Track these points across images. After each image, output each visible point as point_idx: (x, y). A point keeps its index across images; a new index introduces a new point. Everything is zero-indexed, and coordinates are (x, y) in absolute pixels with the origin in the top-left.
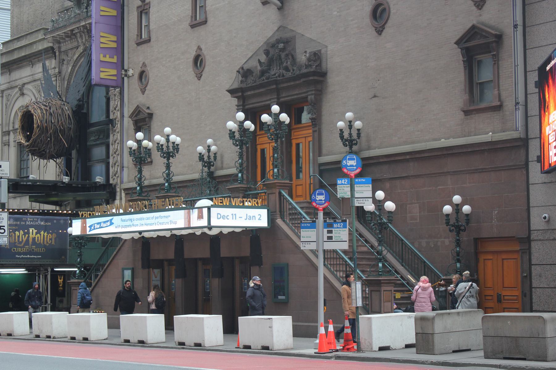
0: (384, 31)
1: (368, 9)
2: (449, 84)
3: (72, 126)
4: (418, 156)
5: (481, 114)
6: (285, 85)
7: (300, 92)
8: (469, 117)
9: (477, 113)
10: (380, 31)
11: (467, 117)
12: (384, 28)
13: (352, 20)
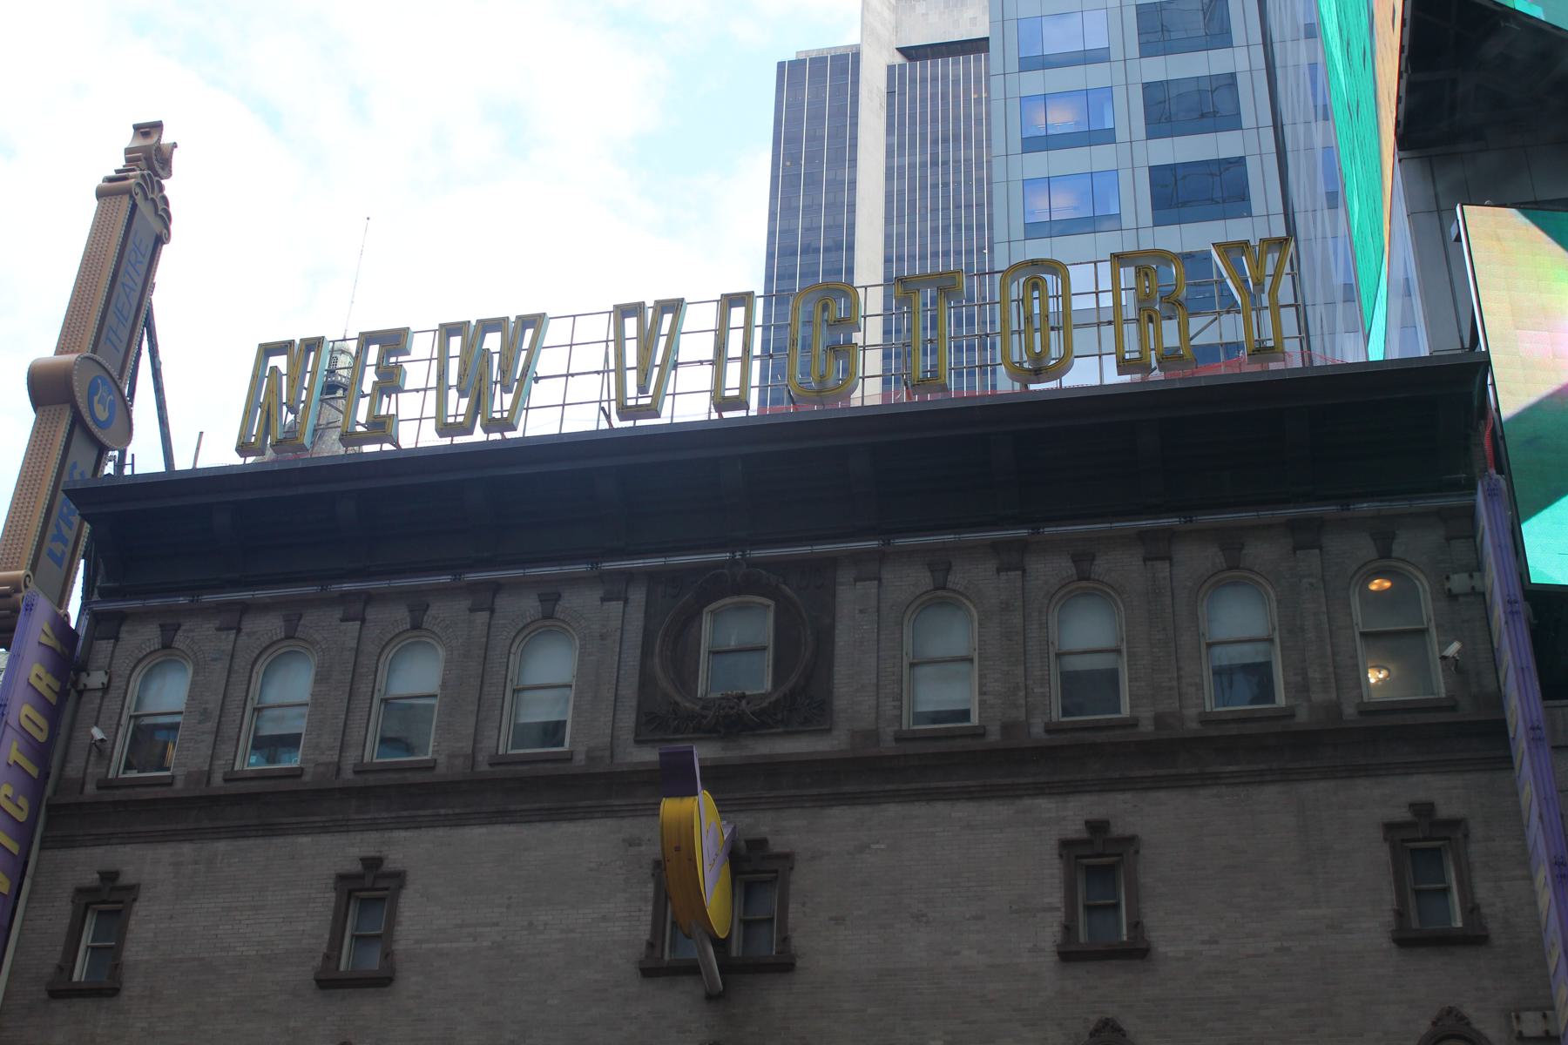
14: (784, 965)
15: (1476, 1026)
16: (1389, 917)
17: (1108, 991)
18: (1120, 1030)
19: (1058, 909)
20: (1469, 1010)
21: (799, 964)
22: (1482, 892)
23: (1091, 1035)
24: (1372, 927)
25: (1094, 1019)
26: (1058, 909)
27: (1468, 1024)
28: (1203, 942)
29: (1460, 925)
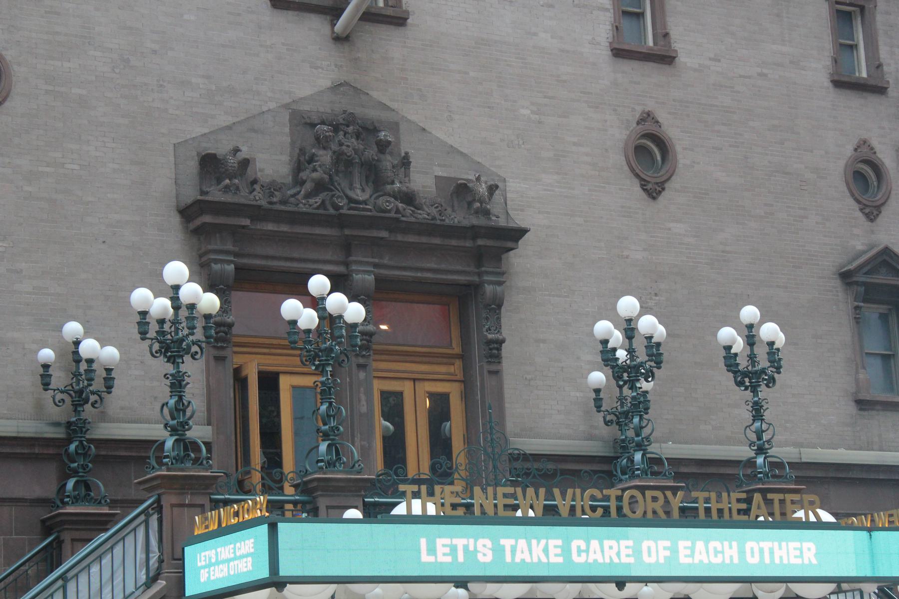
0: (663, 193)
1: (618, 133)
2: (819, 341)
3: (447, 221)
4: (723, 470)
5: (889, 414)
6: (411, 238)
7: (443, 266)
8: (866, 413)
9: (884, 410)
10: (653, 191)
11: (862, 413)
12: (663, 189)
13: (575, 144)
14: (399, 21)
15: (879, 155)
16: (828, 62)
17: (645, 86)
18: (657, 122)
19: (607, 10)
20: (875, 143)
21: (409, 21)
22: (884, 53)
23: (638, 123)
24: (818, 69)
25: (639, 109)
26: (607, 10)
27: (875, 153)
28: (710, 59)
29: (864, 75)
